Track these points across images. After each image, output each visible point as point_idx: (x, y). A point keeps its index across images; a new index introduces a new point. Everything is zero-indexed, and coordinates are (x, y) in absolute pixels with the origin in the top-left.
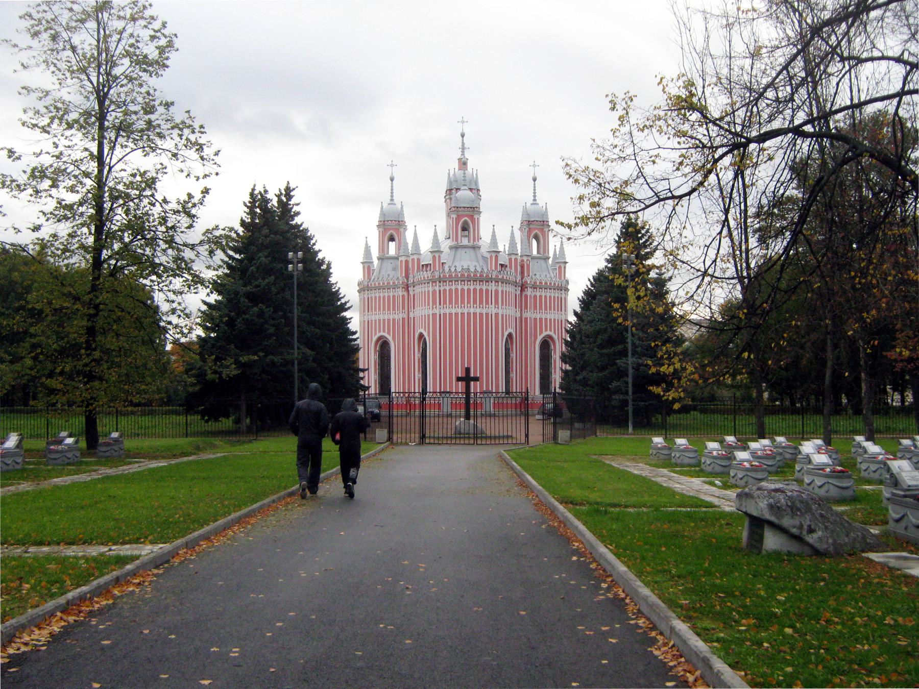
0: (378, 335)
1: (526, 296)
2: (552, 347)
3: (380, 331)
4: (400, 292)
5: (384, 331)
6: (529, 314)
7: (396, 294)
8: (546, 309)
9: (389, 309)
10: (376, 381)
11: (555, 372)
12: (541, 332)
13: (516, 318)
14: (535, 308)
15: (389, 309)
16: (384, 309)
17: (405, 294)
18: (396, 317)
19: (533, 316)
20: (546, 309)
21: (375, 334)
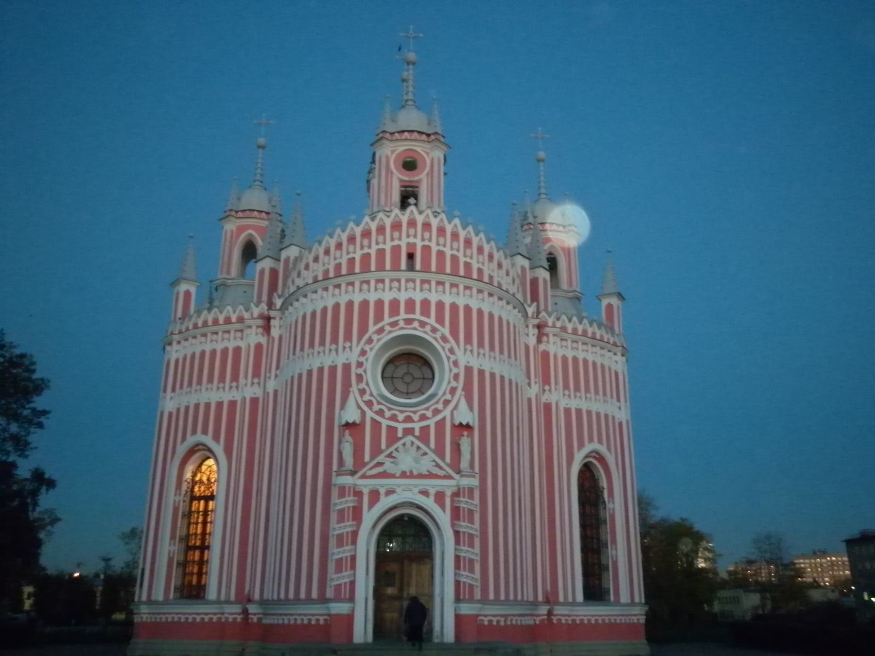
0: (191, 440)
1: (545, 355)
2: (604, 483)
3: (194, 432)
4: (254, 337)
5: (205, 432)
6: (556, 397)
7: (243, 345)
8: (587, 390)
9: (222, 379)
10: (170, 560)
11: (614, 542)
12: (581, 445)
13: (529, 400)
14: (566, 386)
15: (222, 379)
16: (210, 380)
17: (263, 340)
18: (236, 395)
19: (564, 403)
20: (587, 390)
21: (184, 438)
